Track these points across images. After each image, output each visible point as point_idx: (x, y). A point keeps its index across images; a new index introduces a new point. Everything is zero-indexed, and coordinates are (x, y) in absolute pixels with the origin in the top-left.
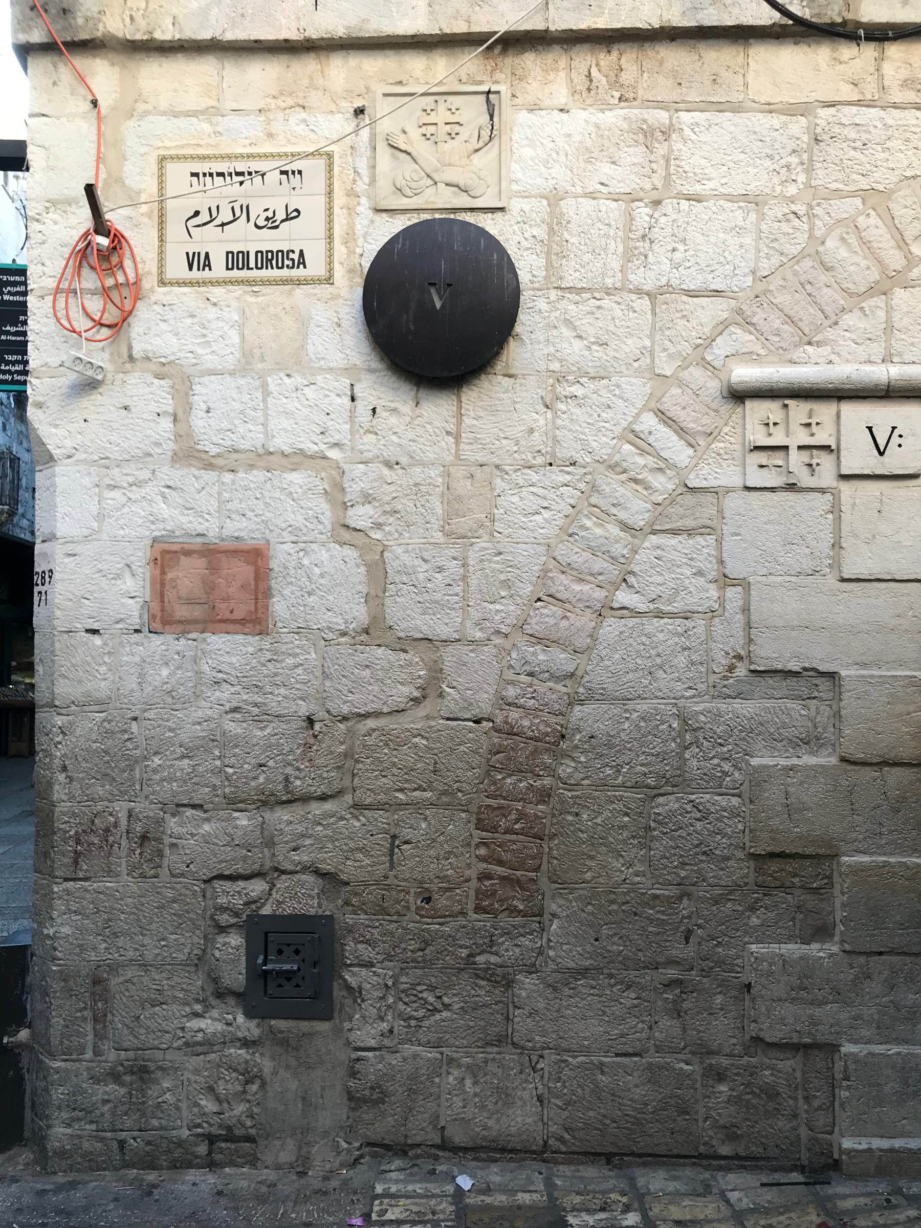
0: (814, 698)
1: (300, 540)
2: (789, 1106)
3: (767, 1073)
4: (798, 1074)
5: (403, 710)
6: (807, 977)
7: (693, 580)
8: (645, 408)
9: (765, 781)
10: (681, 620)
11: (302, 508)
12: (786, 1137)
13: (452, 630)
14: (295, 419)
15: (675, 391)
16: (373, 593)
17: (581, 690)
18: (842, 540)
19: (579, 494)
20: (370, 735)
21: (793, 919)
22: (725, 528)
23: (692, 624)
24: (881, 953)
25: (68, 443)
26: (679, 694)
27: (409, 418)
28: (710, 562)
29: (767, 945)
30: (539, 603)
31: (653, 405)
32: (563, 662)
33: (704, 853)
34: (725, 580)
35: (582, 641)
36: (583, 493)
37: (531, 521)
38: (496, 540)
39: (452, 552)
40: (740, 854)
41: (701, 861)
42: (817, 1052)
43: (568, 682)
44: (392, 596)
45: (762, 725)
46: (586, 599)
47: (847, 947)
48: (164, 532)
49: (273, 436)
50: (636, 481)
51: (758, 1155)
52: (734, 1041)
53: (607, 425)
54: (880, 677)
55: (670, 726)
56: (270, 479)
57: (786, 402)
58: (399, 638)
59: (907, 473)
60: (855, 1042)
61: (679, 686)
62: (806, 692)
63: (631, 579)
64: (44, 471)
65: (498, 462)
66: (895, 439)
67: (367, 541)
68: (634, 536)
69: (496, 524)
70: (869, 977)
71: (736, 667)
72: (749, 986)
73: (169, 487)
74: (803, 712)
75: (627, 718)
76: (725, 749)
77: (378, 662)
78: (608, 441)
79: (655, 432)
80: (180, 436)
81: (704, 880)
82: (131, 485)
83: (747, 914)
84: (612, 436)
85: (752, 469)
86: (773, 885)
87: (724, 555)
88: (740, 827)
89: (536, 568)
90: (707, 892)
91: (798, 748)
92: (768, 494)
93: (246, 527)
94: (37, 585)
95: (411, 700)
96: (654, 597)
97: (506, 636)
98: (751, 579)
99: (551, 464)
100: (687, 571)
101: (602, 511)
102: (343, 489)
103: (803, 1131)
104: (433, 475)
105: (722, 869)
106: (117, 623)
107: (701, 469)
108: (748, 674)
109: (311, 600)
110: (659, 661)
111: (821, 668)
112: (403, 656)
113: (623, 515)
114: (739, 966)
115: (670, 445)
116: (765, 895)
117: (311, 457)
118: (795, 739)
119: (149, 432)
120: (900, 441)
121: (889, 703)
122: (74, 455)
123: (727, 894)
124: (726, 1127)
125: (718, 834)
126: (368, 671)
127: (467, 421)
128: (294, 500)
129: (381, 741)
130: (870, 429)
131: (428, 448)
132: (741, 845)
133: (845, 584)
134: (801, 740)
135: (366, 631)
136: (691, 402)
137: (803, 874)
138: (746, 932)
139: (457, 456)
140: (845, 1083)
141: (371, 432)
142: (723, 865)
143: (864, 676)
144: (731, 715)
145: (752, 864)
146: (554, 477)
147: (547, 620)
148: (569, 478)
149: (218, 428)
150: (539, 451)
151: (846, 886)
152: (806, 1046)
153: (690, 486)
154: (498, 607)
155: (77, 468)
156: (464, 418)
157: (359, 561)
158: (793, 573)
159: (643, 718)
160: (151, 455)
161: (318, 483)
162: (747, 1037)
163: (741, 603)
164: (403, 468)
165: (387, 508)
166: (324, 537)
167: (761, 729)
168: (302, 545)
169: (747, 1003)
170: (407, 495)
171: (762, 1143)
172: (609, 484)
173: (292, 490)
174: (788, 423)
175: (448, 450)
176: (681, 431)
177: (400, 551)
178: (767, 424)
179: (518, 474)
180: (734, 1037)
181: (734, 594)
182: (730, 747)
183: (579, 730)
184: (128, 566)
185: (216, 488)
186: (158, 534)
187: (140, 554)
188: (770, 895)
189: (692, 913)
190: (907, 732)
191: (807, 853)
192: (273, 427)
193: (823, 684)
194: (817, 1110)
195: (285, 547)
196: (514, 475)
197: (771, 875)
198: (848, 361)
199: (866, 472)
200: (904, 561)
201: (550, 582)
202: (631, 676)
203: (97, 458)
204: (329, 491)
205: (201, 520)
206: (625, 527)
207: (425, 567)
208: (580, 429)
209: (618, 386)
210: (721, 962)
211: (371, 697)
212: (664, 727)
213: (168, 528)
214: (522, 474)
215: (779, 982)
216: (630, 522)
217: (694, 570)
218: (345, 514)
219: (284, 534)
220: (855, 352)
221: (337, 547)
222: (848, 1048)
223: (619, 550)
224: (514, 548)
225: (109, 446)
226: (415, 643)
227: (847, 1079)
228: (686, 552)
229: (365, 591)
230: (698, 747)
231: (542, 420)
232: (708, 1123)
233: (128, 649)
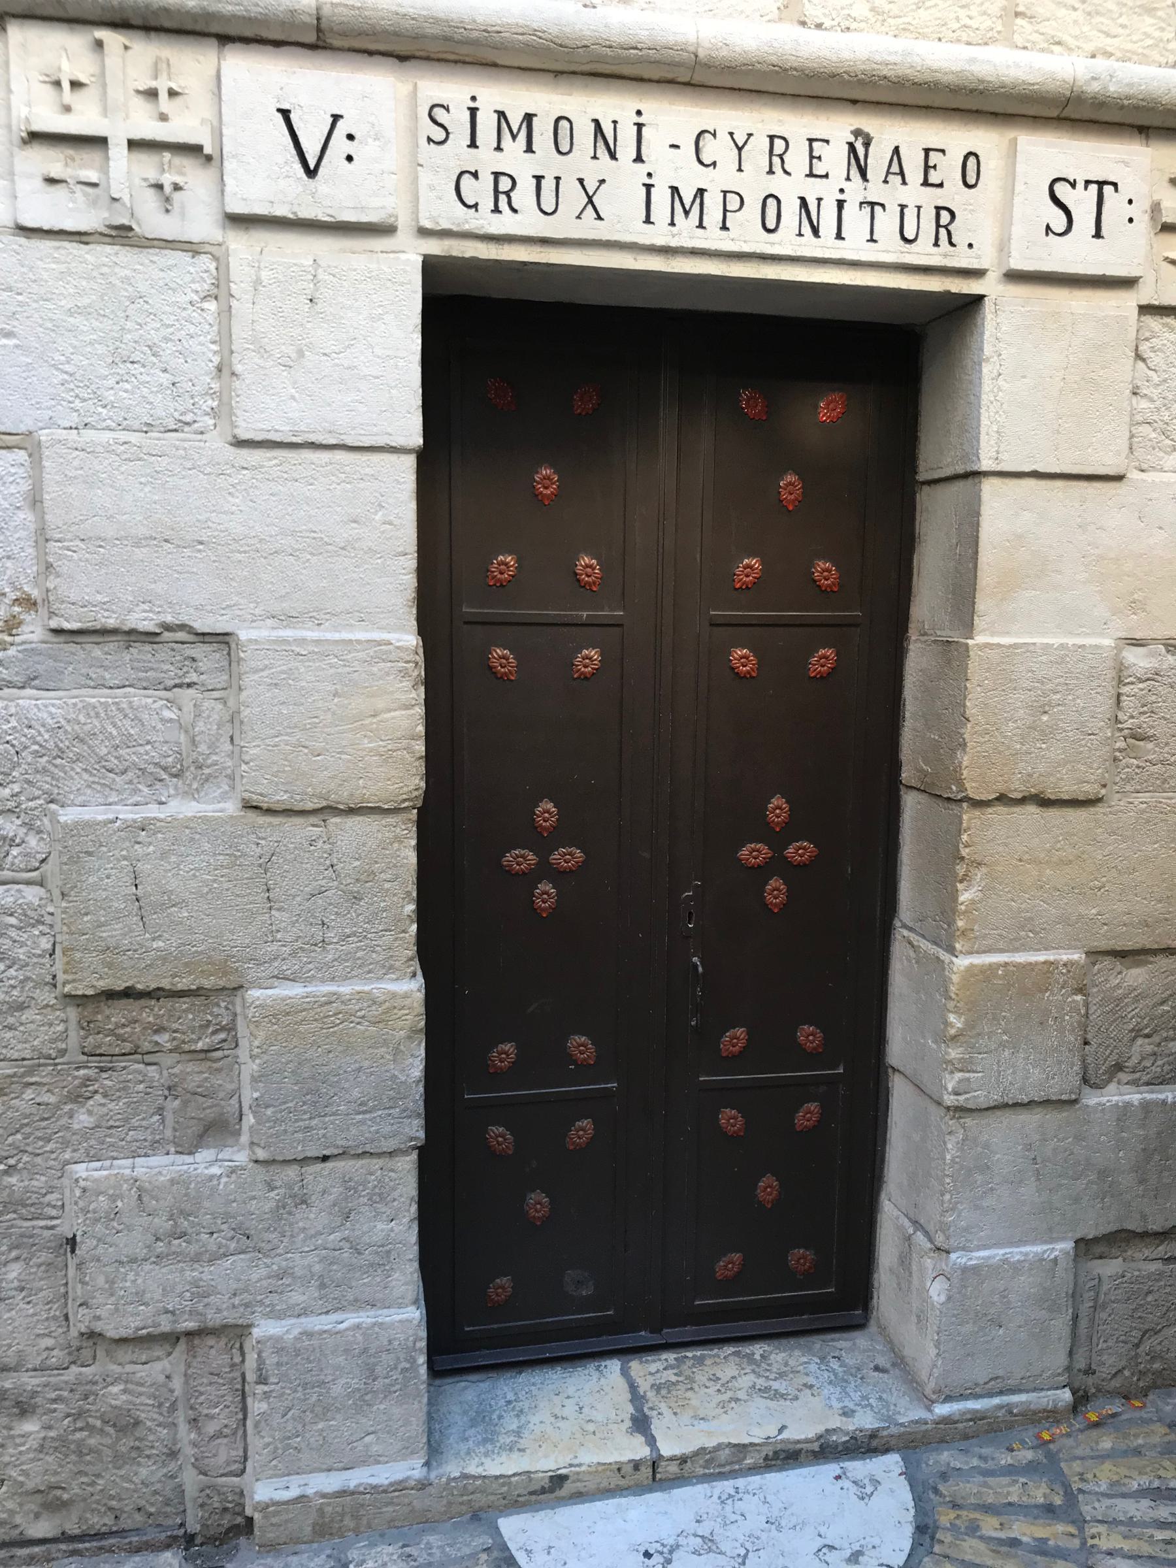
0: (189, 685)
3: (115, 1389)
4: (177, 1384)
6: (186, 1214)
9: (89, 854)
12: (156, 1493)
18: (235, 358)
21: (160, 1110)
24: (325, 1158)
29: (108, 1163)
40: (46, 996)
42: (211, 1341)
45: (82, 741)
47: (261, 1154)
51: (104, 1529)
54: (318, 642)
59: (364, 218)
60: (279, 1316)
62: (171, 674)
66: (339, 143)
70: (304, 1202)
71: (20, 623)
72: (72, 1242)
83: (67, 1108)
86: (117, 1051)
88: (45, 944)
91: (158, 785)
92: (73, 248)
98: (44, 435)
111: (199, 626)
114: (54, 1207)
116: (102, 1070)
118: (151, 768)
121: (336, 694)
123: (23, 1075)
124: (39, 1491)
130: (285, 113)
132: (49, 979)
133: (244, 452)
134: (165, 769)
137: (175, 1026)
138: (66, 1144)
140: (260, 1389)
142: (11, 1020)
143: (284, 641)
144: (14, 723)
145: (72, 1013)
151: (256, 1043)
152: (189, 1334)
158: (136, 425)
162: (74, 1333)
163: (25, 486)
169: (71, 1272)
171: (111, 1509)
174: (104, 86)
178: (57, 84)
180: (48, 1335)
182: (16, 788)
191: (180, 987)
193: (208, 657)
194: (212, 1438)
197: (112, 1032)
199: (280, 211)
200: (364, 409)
215: (130, 1228)
222: (265, 1329)
227: (262, 1380)
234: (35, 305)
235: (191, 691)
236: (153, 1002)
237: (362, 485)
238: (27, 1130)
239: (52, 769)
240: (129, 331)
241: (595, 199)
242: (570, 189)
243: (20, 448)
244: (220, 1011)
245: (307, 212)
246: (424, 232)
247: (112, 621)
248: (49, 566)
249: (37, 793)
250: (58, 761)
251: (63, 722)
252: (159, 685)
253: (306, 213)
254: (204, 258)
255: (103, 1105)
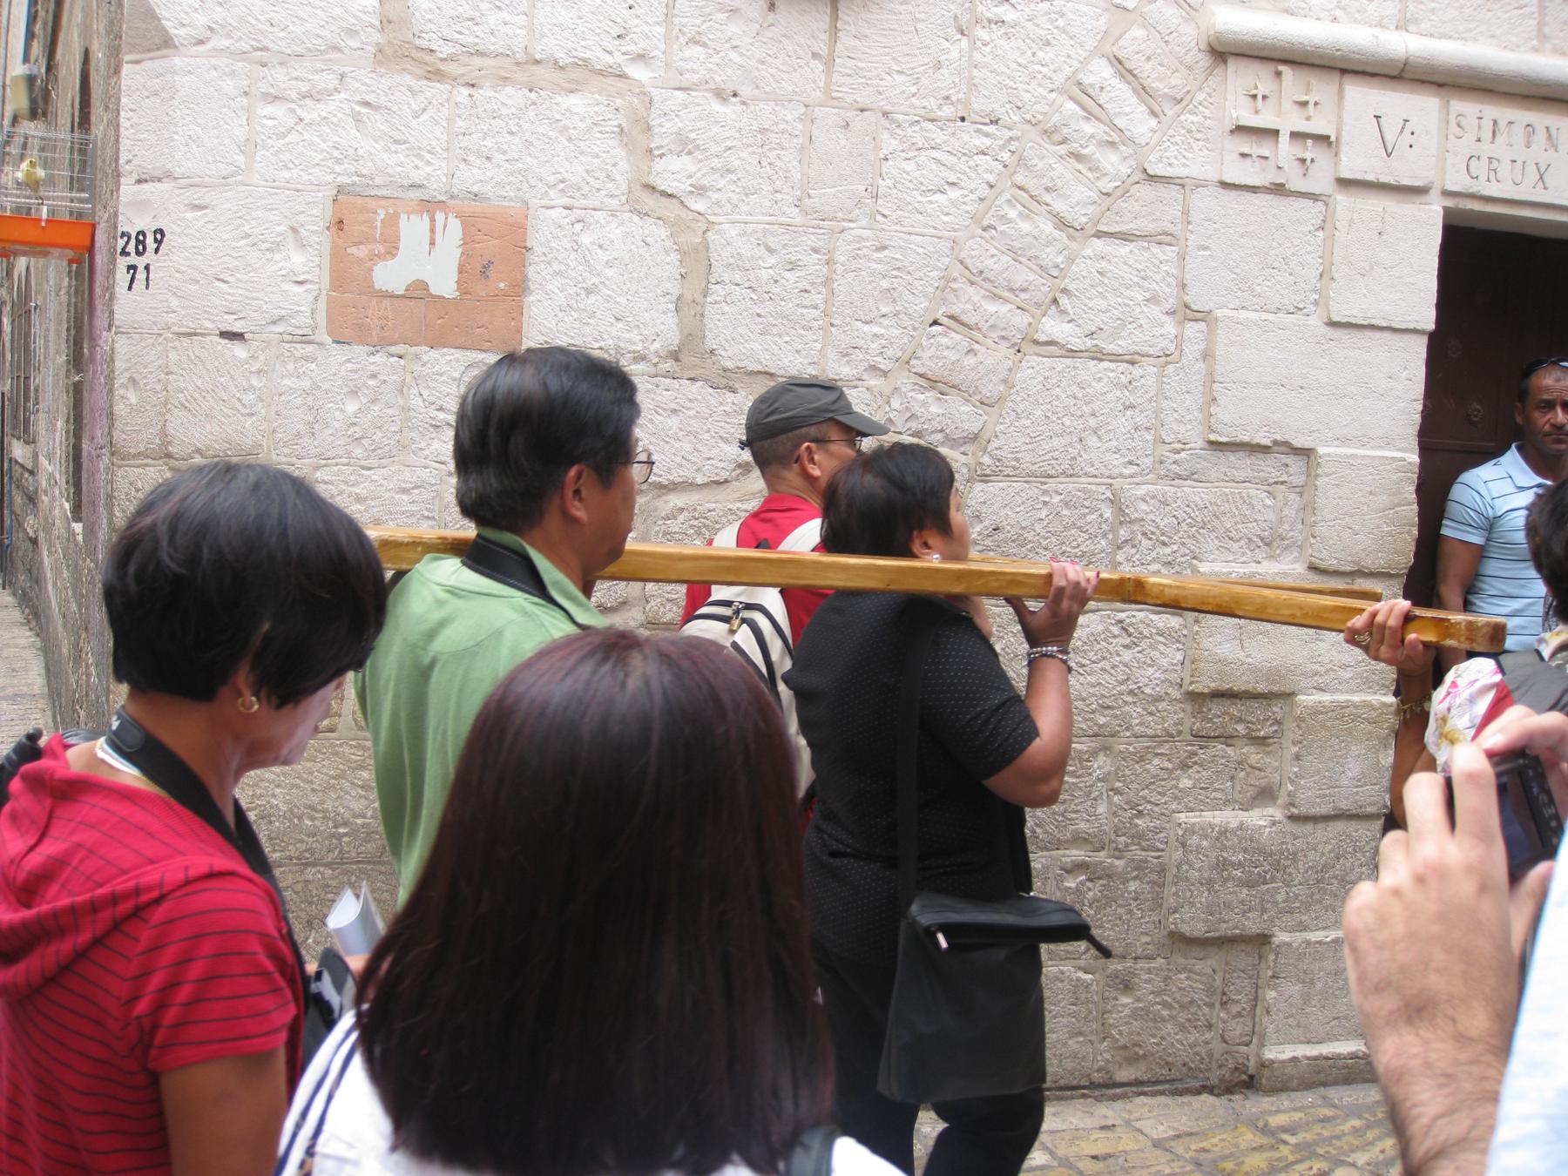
0: (1283, 483)
1: (577, 204)
2: (1204, 1015)
3: (1182, 976)
5: (726, 481)
7: (1145, 309)
8: (1097, 52)
10: (1125, 364)
11: (582, 153)
13: (806, 361)
14: (579, 10)
15: (1138, 32)
16: (688, 297)
17: (986, 460)
19: (1000, 167)
20: (675, 518)
22: (1191, 237)
23: (1137, 371)
25: (201, 20)
26: (1116, 471)
27: (757, 26)
28: (1169, 285)
29: (1198, 813)
30: (935, 328)
31: (1108, 49)
32: (965, 417)
33: (1131, 692)
34: (1187, 313)
35: (992, 389)
36: (1005, 166)
37: (930, 202)
38: (880, 227)
39: (812, 241)
40: (1176, 694)
41: (1126, 702)
43: (968, 448)
44: (716, 302)
45: (1217, 517)
46: (1003, 325)
48: (356, 179)
49: (543, 35)
50: (1078, 157)
51: (1162, 1078)
52: (1147, 939)
53: (1045, 70)
54: (1364, 457)
55: (1101, 515)
56: (534, 103)
57: (1281, 68)
58: (725, 370)
61: (1117, 460)
62: (1274, 475)
63: (1064, 301)
64: (147, 65)
65: (888, 108)
67: (683, 213)
68: (1071, 238)
69: (880, 202)
73: (367, 104)
74: (1268, 502)
75: (1045, 503)
76: (1168, 550)
77: (689, 405)
78: (1045, 93)
79: (1108, 89)
80: (390, 22)
81: (1127, 729)
82: (304, 97)
84: (1051, 86)
85: (1231, 158)
87: (1187, 276)
88: (1179, 656)
89: (935, 274)
90: (1130, 744)
93: (492, 178)
94: (128, 254)
95: (739, 466)
96: (1094, 329)
97: (885, 374)
98: (1219, 313)
99: (963, 119)
100: (1138, 295)
101: (1031, 197)
102: (649, 129)
103: (1218, 1047)
104: (790, 118)
105: (1151, 714)
106: (274, 323)
107: (1166, 150)
108: (1206, 446)
109: (590, 301)
110: (1093, 422)
111: (1297, 443)
112: (730, 397)
113: (1059, 206)
114: (1162, 843)
115: (1127, 109)
117: (601, 73)
118: (1255, 539)
119: (339, 11)
120: (1411, 140)
122: (208, 39)
125: (1149, 665)
126: (674, 418)
127: (845, 40)
128: (570, 139)
129: (692, 526)
131: (785, 76)
132: (1179, 680)
134: (1262, 539)
135: (675, 356)
136: (1159, 51)
139: (827, 91)
141: (697, 43)
144: (1179, 503)
145: (1188, 707)
146: (966, 138)
147: (945, 353)
148: (987, 141)
149: (454, 13)
150: (947, 98)
153: (1151, 172)
154: (876, 329)
155: (214, 61)
156: (840, 34)
157: (668, 244)
158: (1272, 308)
159: (1067, 504)
160: (336, 49)
161: (610, 116)
162: (1164, 932)
163: (1203, 346)
164: (744, 103)
165: (716, 163)
166: (615, 202)
167: (1216, 523)
168: (579, 213)
170: (749, 146)
171: (1167, 1063)
172: (1042, 158)
173: (567, 122)
175: (815, 82)
176: (1144, 92)
177: (733, 233)
179: (916, 128)
180: (1146, 934)
181: (1193, 330)
182: (1175, 547)
183: (978, 518)
184: (294, 230)
185: (445, 111)
186: (349, 181)
187: (315, 211)
188: (1206, 747)
189: (1109, 773)
190: (1388, 532)
192: (543, 20)
193: (1297, 465)
195: (553, 213)
196: (910, 130)
198: (1355, 21)
199: (1370, 177)
201: (951, 297)
202: (1056, 442)
203: (247, 48)
204: (626, 129)
205: (417, 162)
206: (1062, 224)
207: (772, 260)
208: (1008, 71)
209: (1062, 15)
210: (1139, 837)
211: (678, 459)
212: (1094, 517)
213: (364, 171)
214: (921, 129)
216: (1069, 217)
217: (1147, 295)
218: (650, 167)
219: (551, 192)
220: (1366, 11)
221: (636, 219)
223: (1051, 256)
224: (905, 241)
225: (270, 29)
226: (747, 379)
228: (1140, 267)
229: (676, 292)
230: (1134, 546)
231: (956, 49)
232: (1105, 1044)
233: (291, 367)
234: (1223, 231)
235: (1283, 487)
236: (1238, 701)
237: (1397, 354)
238: (1153, 787)
239: (1198, 536)
240: (1274, 249)
241: (1545, 177)
242: (1531, 169)
243: (1203, 321)
244: (1277, 709)
245: (1385, 179)
246: (1446, 193)
247: (1246, 437)
248: (1215, 399)
249: (1188, 551)
250: (1201, 531)
251: (1208, 504)
252: (1264, 482)
253: (1384, 179)
254: (1320, 204)
255: (1198, 772)
